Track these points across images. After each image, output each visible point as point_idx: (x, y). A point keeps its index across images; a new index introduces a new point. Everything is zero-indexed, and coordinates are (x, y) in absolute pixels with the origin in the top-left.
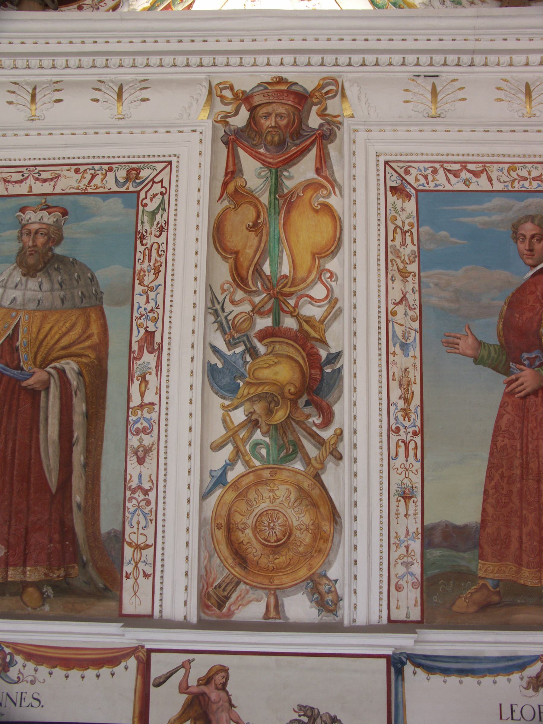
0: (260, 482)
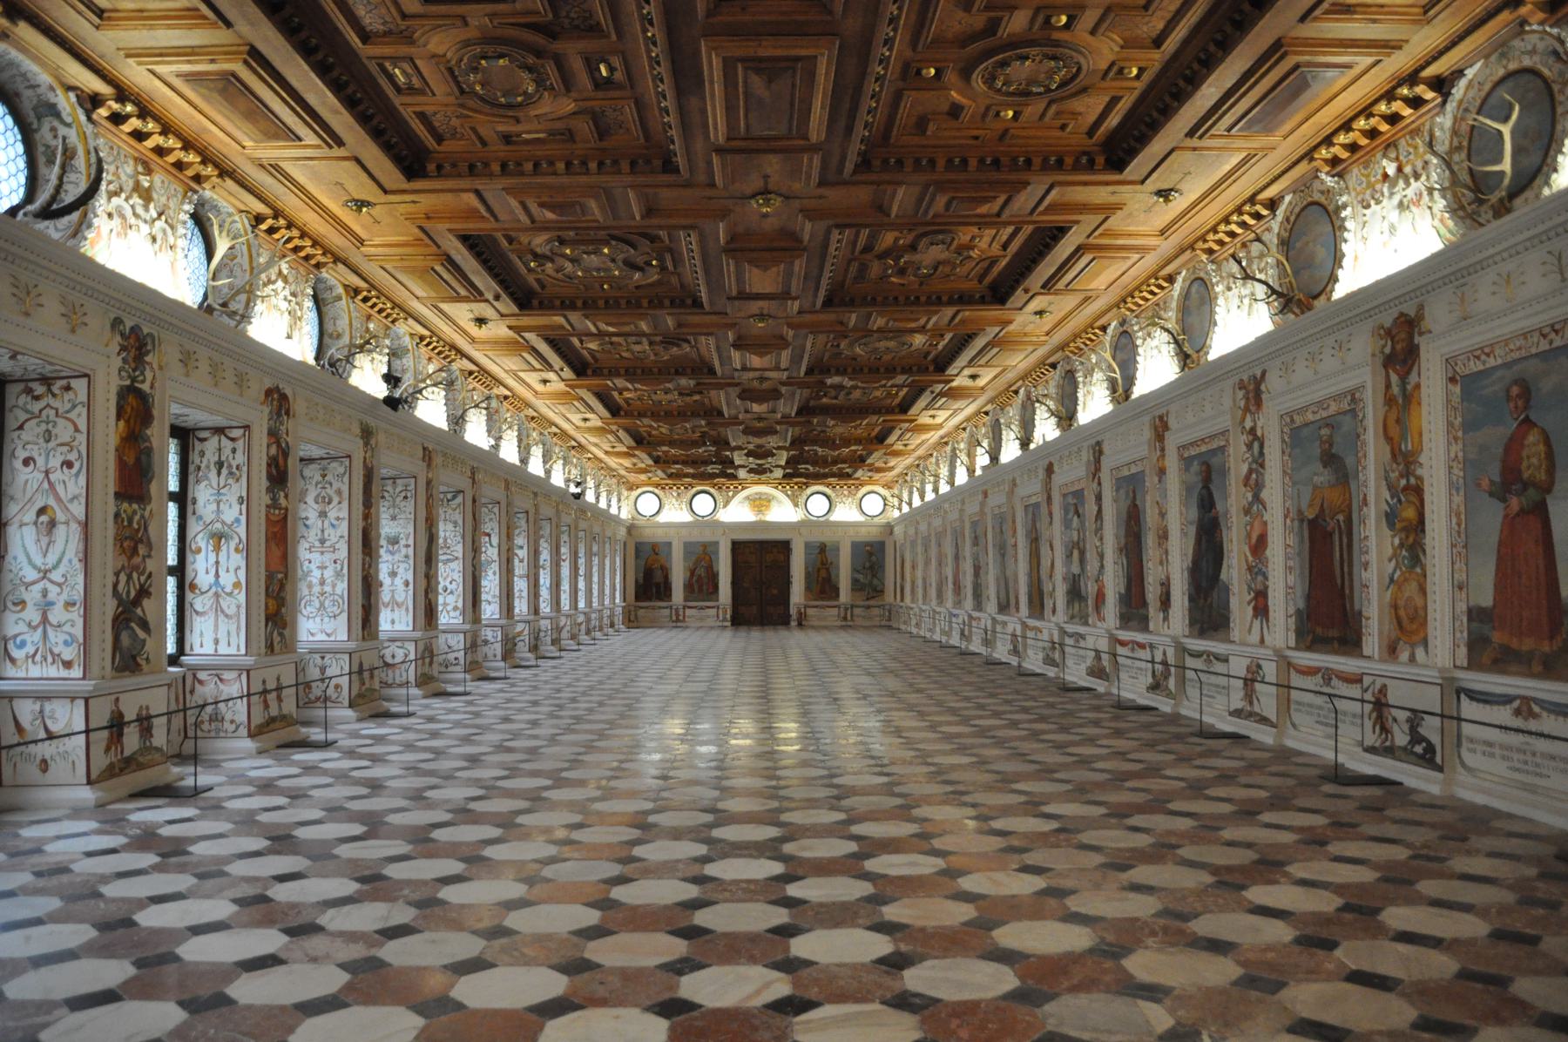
0: (1406, 580)
